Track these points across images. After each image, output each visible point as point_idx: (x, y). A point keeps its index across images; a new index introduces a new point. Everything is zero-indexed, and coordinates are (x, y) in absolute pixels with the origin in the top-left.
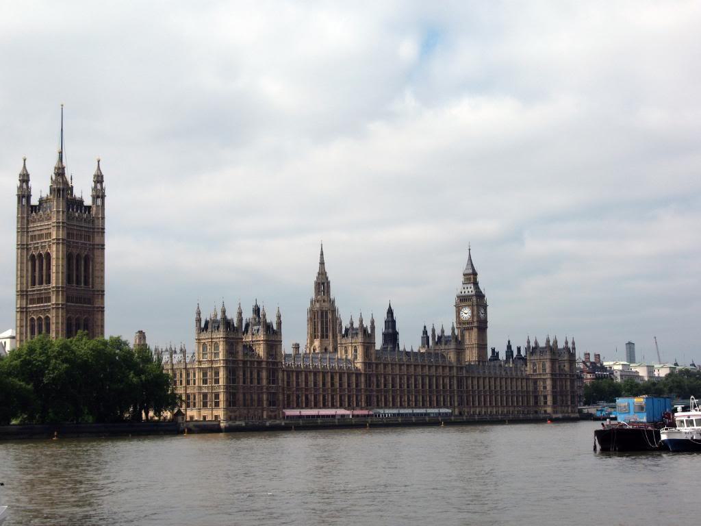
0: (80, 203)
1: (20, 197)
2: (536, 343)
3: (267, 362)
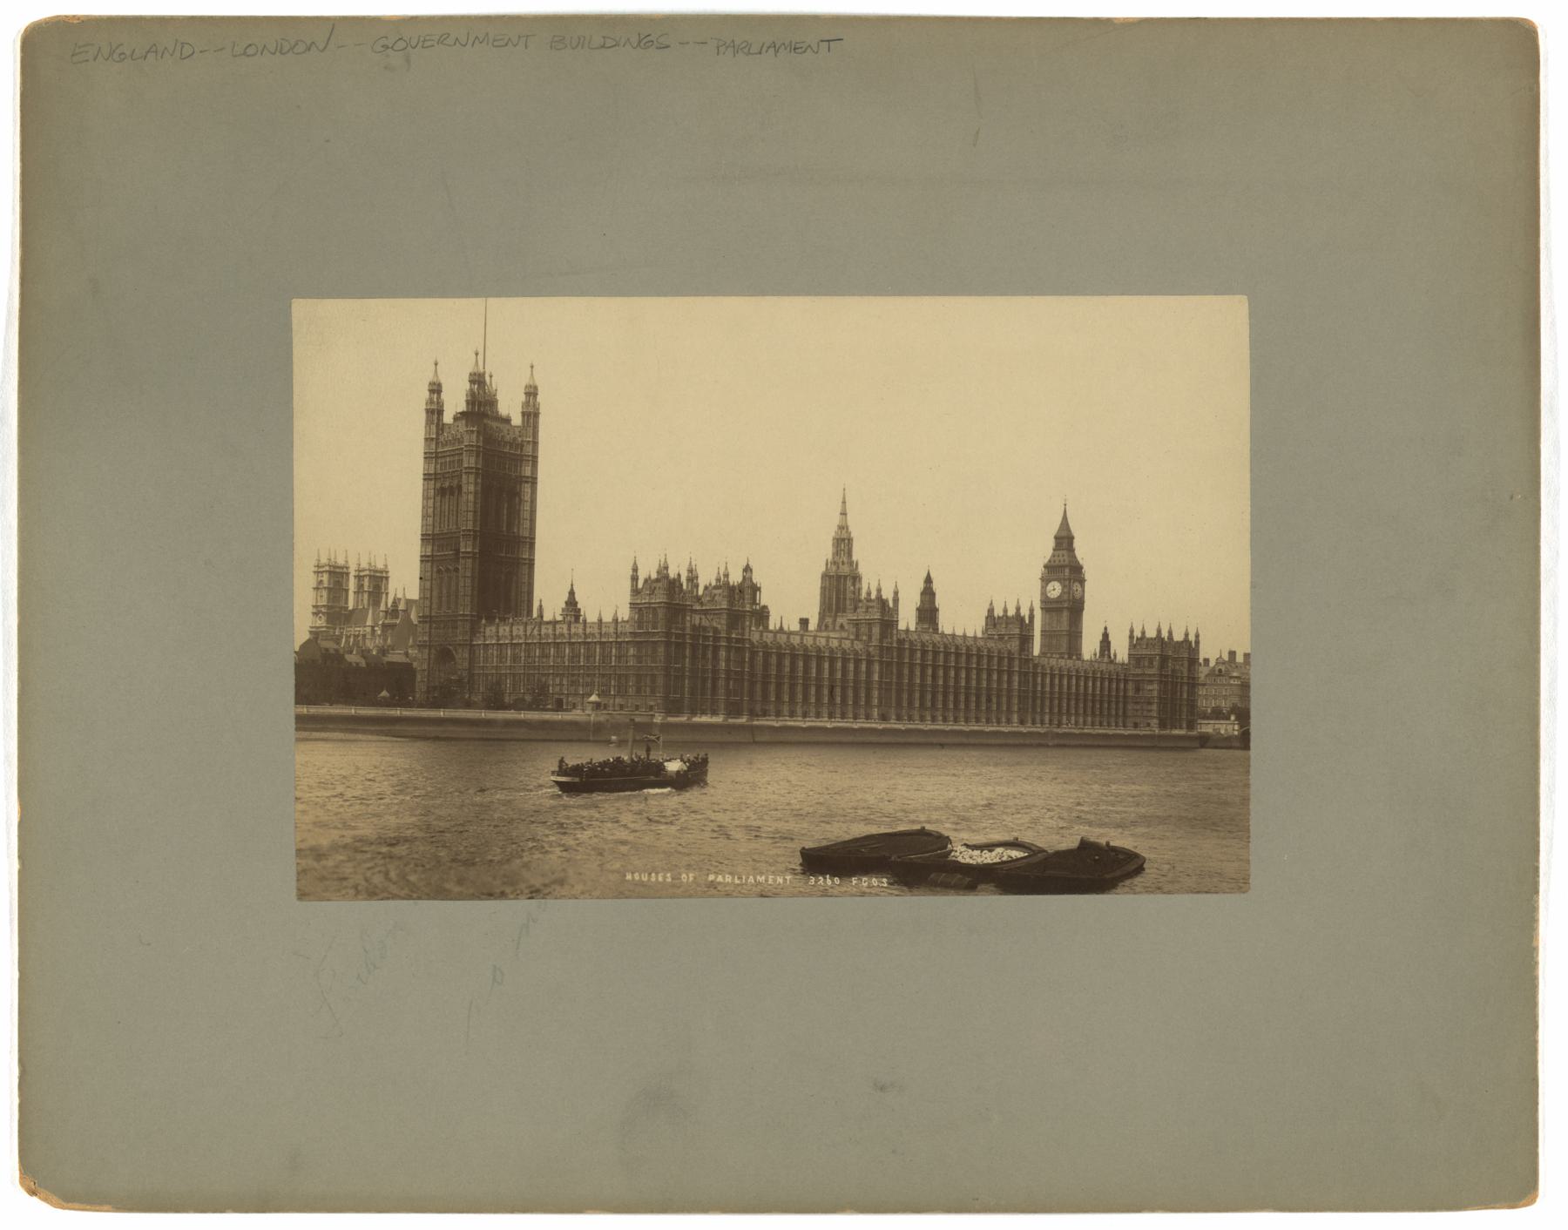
0: (507, 420)
1: (429, 412)
2: (1143, 633)
3: (729, 640)
